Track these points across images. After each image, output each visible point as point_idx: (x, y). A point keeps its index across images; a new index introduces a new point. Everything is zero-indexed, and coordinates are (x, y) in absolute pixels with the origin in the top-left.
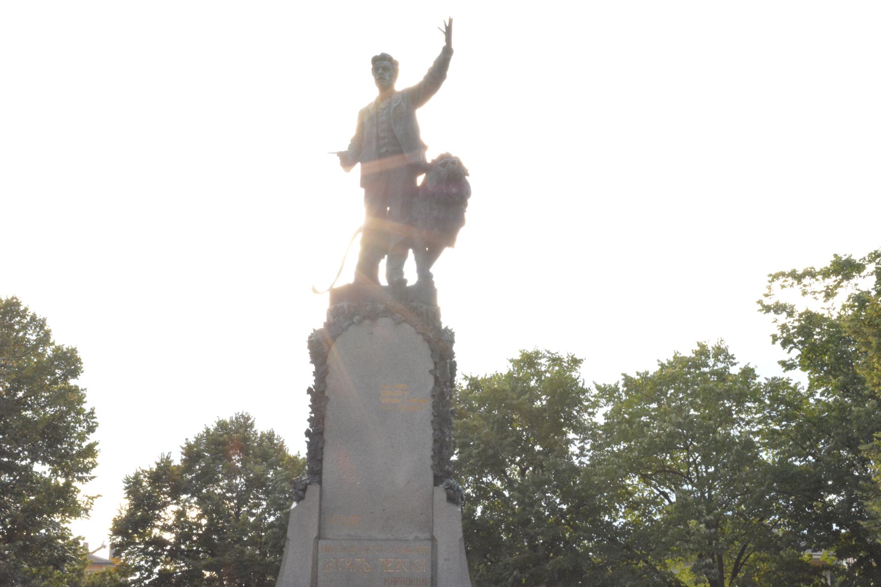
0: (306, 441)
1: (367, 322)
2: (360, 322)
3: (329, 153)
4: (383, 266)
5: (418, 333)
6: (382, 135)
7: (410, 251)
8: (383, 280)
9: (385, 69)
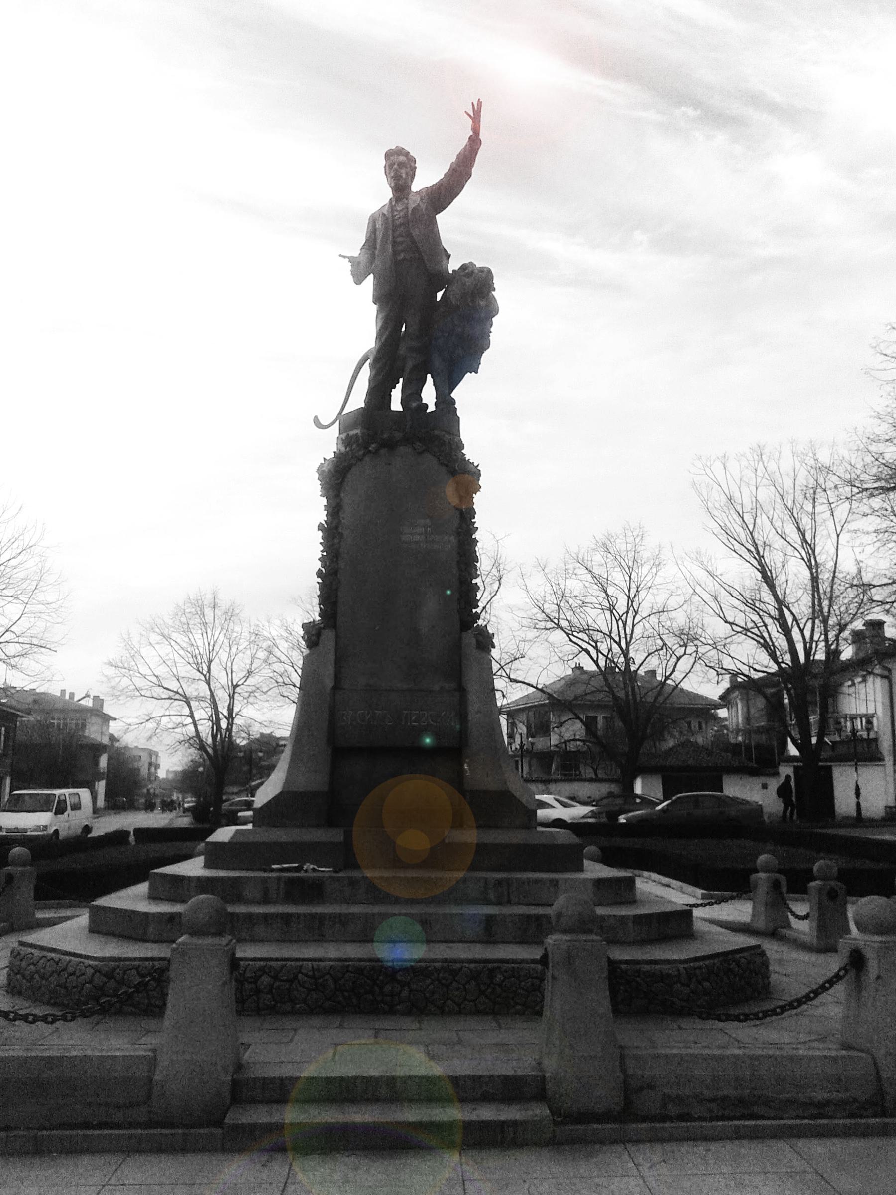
0: (318, 583)
1: (383, 451)
2: (376, 452)
3: (340, 256)
4: (396, 395)
5: (442, 464)
6: (399, 239)
7: (429, 376)
8: (396, 405)
9: (401, 165)
